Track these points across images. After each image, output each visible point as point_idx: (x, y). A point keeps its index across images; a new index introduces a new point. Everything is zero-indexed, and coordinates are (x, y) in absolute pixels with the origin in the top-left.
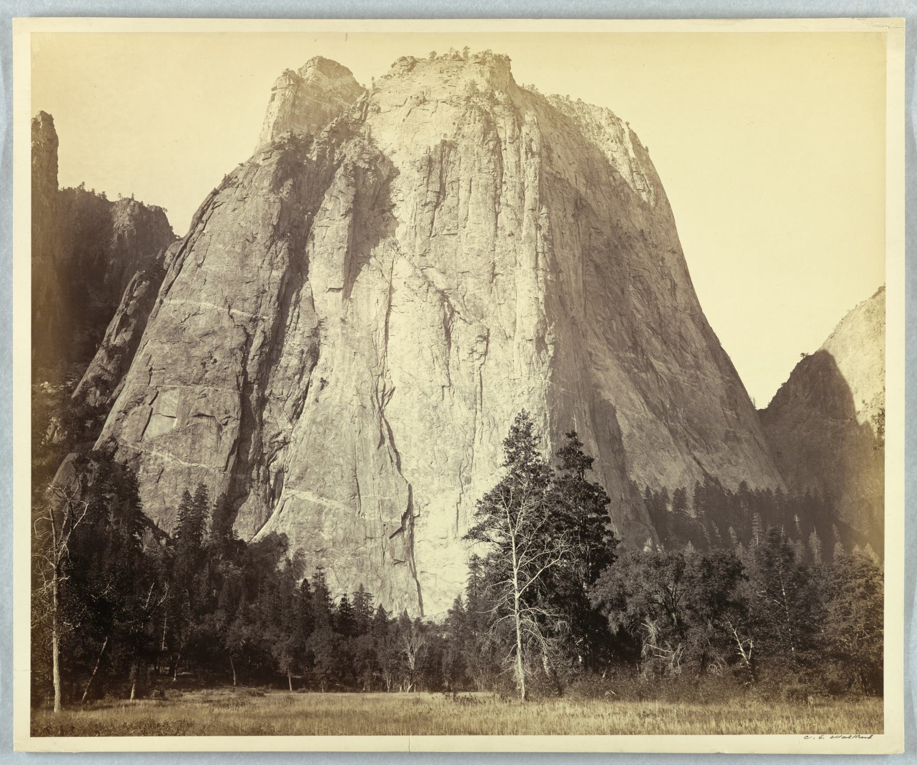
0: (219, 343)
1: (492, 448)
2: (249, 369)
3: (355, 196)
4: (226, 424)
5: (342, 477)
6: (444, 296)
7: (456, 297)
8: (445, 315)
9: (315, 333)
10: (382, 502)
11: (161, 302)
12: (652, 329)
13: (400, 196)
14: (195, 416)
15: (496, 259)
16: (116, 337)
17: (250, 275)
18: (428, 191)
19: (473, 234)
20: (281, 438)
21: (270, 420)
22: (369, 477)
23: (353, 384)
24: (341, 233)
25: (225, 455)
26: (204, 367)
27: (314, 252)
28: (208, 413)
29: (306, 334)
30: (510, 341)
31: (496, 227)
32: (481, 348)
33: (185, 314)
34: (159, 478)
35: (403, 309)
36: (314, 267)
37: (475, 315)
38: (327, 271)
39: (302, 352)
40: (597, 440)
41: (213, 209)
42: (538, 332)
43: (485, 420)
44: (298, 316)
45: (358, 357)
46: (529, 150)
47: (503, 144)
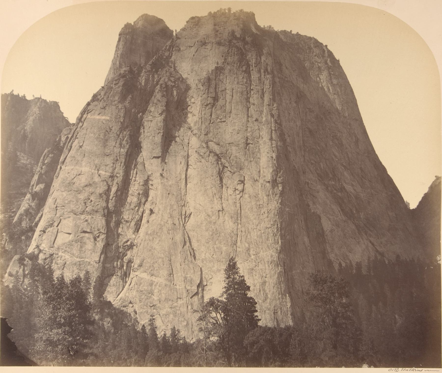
0: (93, 191)
1: (247, 245)
2: (109, 206)
3: (167, 102)
4: (98, 237)
5: (163, 264)
6: (218, 157)
7: (225, 158)
8: (219, 169)
9: (146, 182)
10: (186, 278)
11: (61, 168)
12: (344, 166)
13: (193, 100)
14: (81, 232)
15: (248, 134)
16: (36, 186)
17: (109, 151)
18: (208, 97)
19: (235, 121)
20: (129, 243)
21: (122, 233)
22: (178, 264)
23: (168, 211)
24: (159, 125)
25: (99, 254)
26: (85, 205)
27: (144, 136)
28: (88, 230)
29: (141, 184)
30: (257, 182)
31: (248, 116)
32: (240, 187)
33: (74, 175)
34: (64, 267)
35: (195, 167)
36: (144, 144)
37: (237, 168)
38: (152, 147)
39: (139, 194)
40: (309, 237)
41: (87, 113)
42: (273, 176)
43: (243, 229)
44: (137, 173)
45: (170, 196)
46: (266, 70)
47: (251, 67)
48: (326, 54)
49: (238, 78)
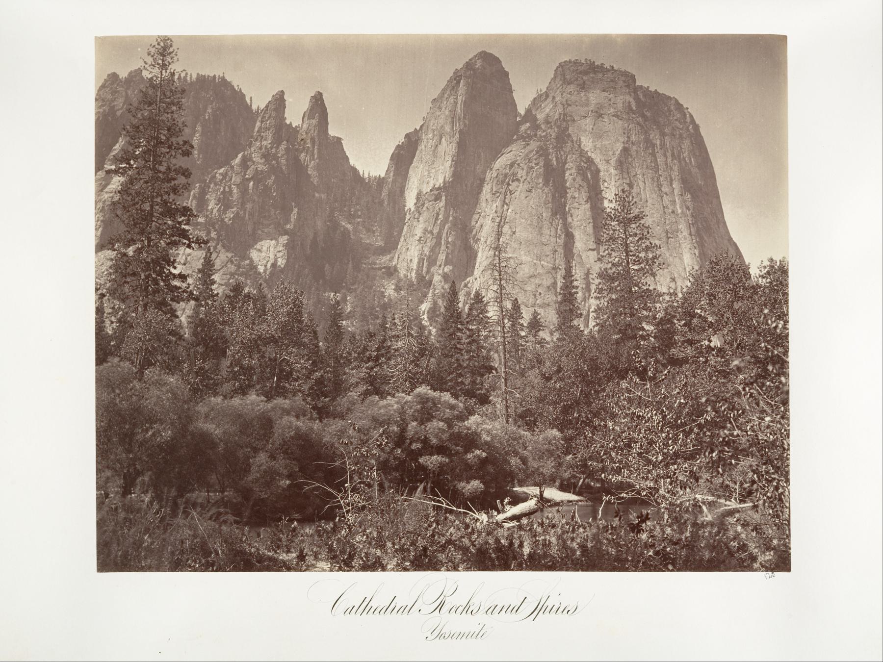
0: (540, 282)
15: (667, 227)
29: (582, 277)
48: (688, 120)
49: (646, 161)
